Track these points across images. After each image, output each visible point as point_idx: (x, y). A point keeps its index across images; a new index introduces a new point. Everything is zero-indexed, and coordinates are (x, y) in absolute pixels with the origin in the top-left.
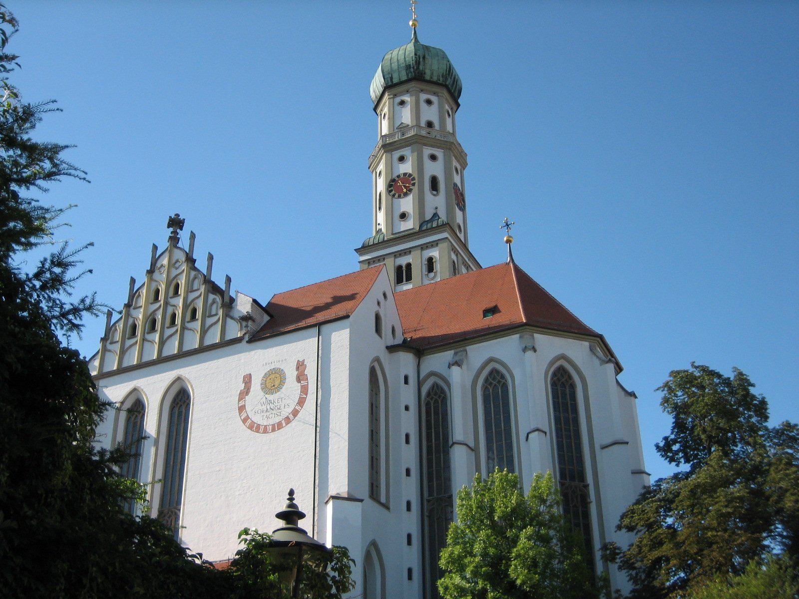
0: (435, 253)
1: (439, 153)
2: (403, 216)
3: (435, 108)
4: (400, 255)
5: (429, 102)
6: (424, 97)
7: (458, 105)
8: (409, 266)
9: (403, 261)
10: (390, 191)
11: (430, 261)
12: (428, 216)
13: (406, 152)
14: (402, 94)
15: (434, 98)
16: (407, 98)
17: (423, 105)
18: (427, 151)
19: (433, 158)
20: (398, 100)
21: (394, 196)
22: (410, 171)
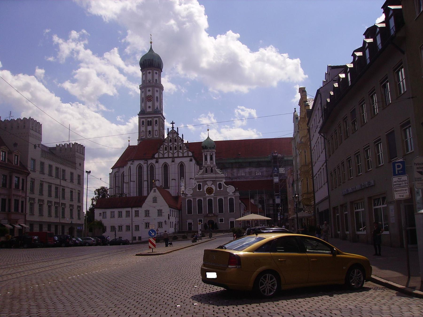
0: (157, 119)
1: (158, 89)
2: (149, 107)
3: (158, 75)
4: (149, 118)
5: (156, 73)
6: (155, 71)
7: (162, 71)
8: (151, 121)
9: (149, 120)
10: (146, 99)
11: (156, 121)
12: (156, 108)
13: (151, 89)
14: (149, 70)
15: (157, 72)
16: (151, 71)
17: (155, 74)
18: (156, 89)
19: (157, 91)
20: (148, 71)
21: (147, 101)
22: (151, 95)
